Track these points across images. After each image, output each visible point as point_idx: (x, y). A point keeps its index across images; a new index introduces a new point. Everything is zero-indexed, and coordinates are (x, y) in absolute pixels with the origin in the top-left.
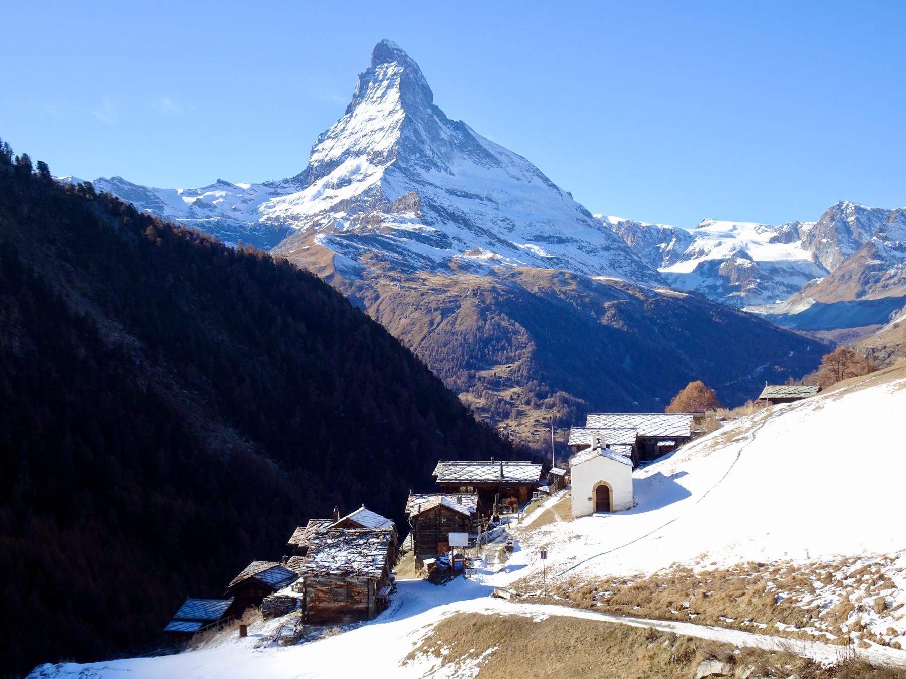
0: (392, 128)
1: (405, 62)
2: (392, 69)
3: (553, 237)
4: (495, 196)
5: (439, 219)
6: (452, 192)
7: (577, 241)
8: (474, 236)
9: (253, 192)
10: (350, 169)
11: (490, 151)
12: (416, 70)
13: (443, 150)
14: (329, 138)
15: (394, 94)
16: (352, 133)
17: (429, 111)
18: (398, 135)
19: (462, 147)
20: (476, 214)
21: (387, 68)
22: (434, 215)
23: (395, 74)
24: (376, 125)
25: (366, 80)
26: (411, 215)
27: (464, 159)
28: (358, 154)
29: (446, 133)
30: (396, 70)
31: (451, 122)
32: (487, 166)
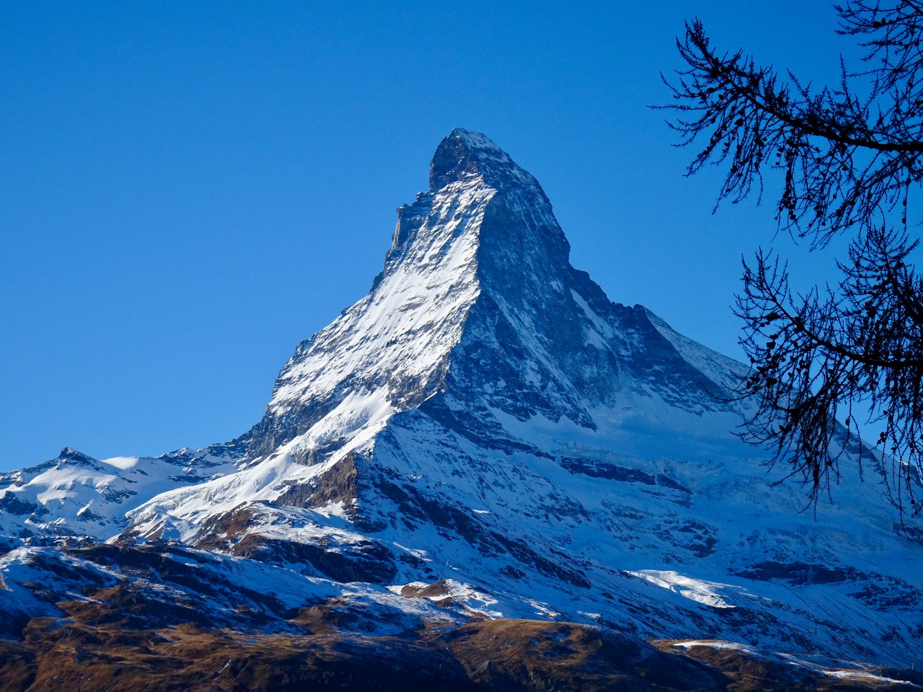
0: (448, 322)
1: (506, 178)
2: (472, 192)
3: (805, 567)
4: (684, 472)
5: (399, 515)
6: (576, 466)
7: (863, 576)
8: (477, 554)
9: (138, 477)
10: (346, 416)
11: (707, 373)
12: (533, 193)
13: (588, 372)
14: (316, 351)
15: (465, 249)
16: (365, 339)
17: (555, 284)
18: (458, 339)
19: (638, 366)
20: (618, 514)
21: (460, 191)
22: (388, 506)
23: (474, 205)
24: (421, 317)
25: (413, 217)
26: (336, 508)
27: (642, 393)
28: (371, 384)
29: (599, 334)
30: (478, 195)
31: (618, 308)
32: (698, 408)
